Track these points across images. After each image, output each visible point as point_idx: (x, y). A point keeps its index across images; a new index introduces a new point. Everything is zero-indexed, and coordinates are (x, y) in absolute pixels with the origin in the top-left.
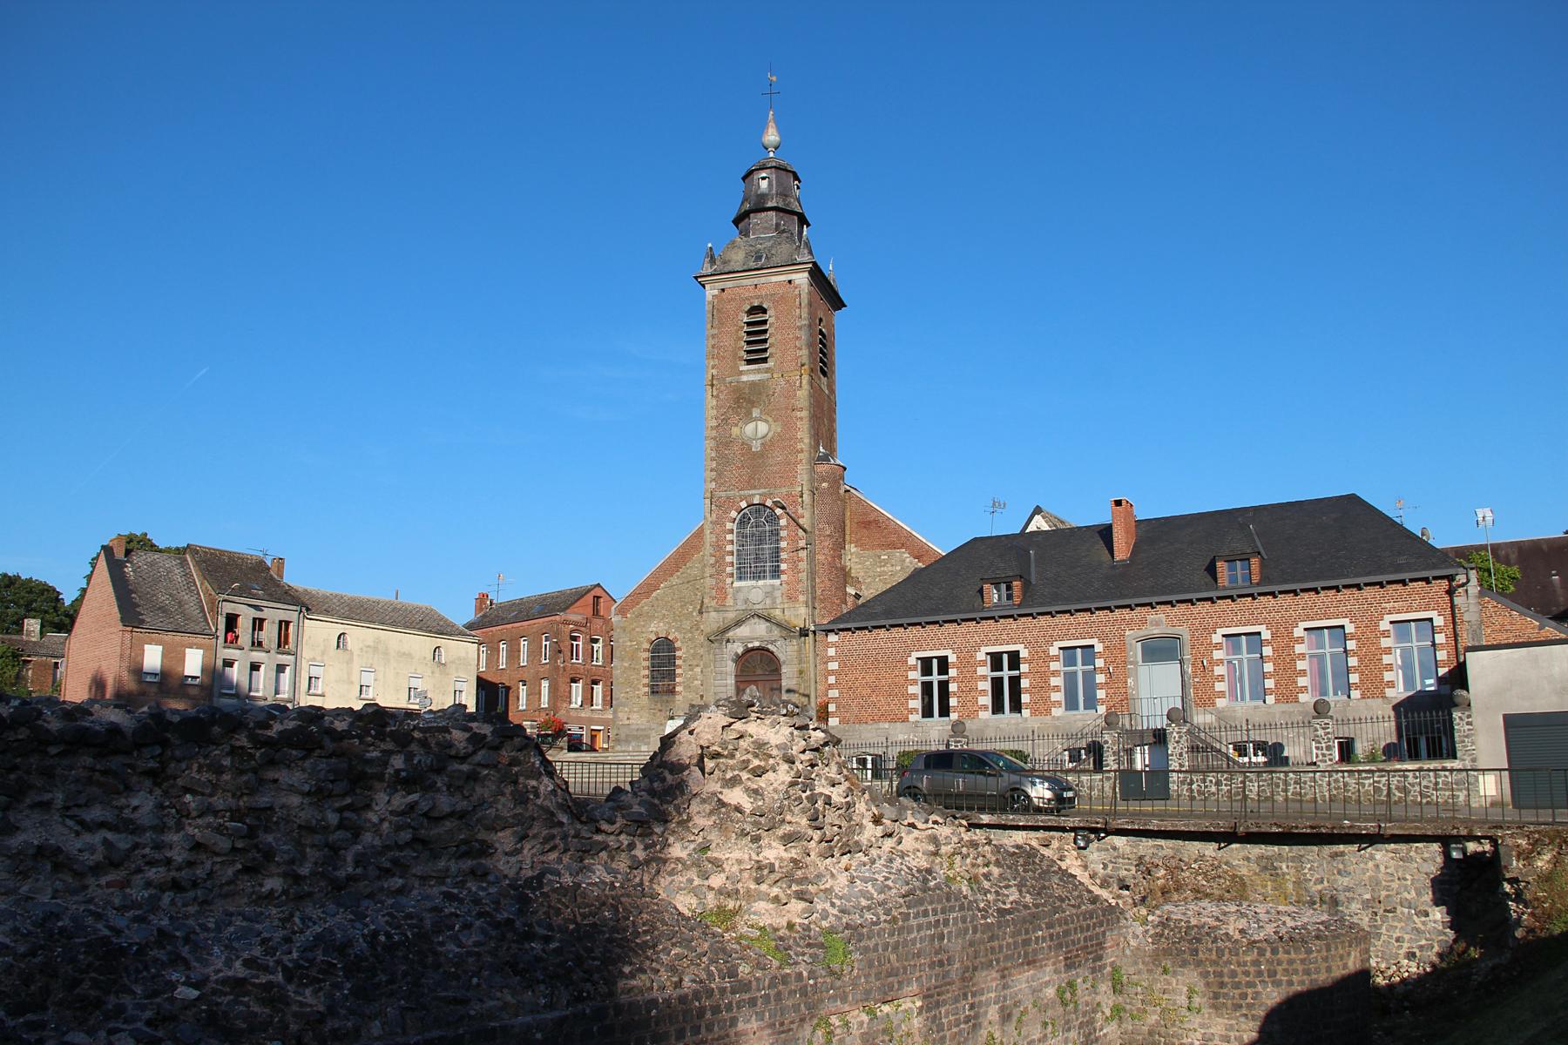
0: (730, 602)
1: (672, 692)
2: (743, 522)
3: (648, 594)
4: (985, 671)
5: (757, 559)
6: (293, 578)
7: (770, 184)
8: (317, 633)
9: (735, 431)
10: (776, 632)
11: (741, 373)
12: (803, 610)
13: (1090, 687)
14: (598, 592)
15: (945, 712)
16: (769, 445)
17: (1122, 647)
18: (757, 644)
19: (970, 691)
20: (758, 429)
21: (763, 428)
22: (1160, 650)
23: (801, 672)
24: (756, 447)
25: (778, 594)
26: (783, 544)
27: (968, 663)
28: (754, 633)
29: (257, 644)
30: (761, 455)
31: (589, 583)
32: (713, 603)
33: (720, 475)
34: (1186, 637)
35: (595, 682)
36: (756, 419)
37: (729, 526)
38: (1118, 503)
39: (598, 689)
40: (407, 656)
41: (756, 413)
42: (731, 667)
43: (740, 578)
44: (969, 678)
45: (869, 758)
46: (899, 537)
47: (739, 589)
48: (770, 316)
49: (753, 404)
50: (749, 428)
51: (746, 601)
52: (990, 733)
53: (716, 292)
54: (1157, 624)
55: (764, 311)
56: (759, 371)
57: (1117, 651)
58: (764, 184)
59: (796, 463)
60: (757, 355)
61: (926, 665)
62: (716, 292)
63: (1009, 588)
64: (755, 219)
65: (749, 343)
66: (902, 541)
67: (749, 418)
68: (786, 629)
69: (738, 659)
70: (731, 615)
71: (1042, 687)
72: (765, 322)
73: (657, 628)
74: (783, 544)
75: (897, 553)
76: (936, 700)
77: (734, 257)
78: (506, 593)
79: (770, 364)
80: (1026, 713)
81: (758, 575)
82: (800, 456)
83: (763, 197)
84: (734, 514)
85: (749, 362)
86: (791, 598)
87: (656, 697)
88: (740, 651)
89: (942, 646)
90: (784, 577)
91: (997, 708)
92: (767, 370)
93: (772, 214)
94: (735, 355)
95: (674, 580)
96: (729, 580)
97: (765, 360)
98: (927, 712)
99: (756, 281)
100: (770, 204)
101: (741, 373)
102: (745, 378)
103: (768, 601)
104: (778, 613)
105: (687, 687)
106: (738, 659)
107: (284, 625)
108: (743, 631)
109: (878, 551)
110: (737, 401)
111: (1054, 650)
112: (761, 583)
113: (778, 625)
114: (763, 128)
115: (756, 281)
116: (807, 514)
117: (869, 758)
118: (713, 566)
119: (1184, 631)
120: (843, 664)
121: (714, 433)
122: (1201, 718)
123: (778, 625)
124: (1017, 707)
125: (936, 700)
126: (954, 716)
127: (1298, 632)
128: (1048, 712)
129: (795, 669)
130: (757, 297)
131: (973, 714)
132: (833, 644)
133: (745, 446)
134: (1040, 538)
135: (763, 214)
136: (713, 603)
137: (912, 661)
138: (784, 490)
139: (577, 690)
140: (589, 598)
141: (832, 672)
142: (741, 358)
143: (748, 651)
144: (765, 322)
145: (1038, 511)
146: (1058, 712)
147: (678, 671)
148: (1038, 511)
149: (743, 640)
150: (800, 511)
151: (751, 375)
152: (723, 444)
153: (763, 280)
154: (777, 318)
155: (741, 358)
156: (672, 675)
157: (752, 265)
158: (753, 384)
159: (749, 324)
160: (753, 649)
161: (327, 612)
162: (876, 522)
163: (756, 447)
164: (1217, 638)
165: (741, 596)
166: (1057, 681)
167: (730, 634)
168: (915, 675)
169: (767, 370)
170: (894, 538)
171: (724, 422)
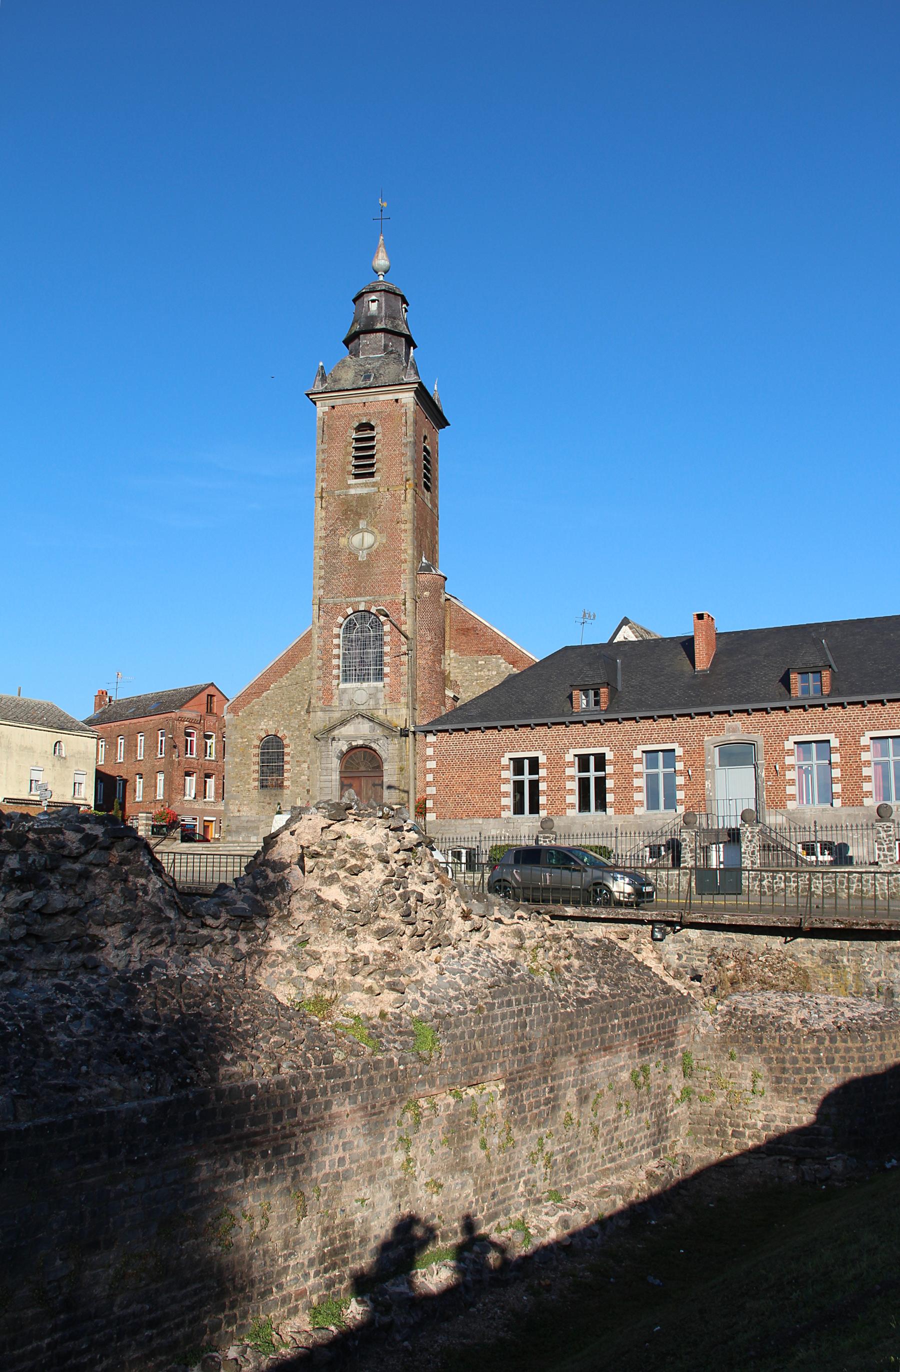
0: (335, 702)
1: (281, 786)
2: (350, 626)
3: (258, 694)
4: (573, 771)
5: (362, 662)
7: (379, 307)
9: (343, 541)
10: (379, 731)
11: (349, 486)
12: (404, 711)
14: (210, 690)
15: (535, 809)
16: (374, 555)
17: (701, 750)
18: (360, 742)
19: (558, 790)
20: (364, 540)
21: (369, 539)
22: (736, 754)
23: (401, 769)
24: (362, 556)
25: (381, 695)
26: (387, 649)
27: (557, 764)
28: (358, 732)
30: (368, 564)
31: (203, 682)
32: (320, 704)
33: (328, 583)
34: (761, 743)
35: (208, 776)
36: (362, 531)
37: (336, 630)
38: (700, 617)
39: (211, 782)
40: (28, 750)
41: (362, 524)
42: (336, 763)
43: (346, 680)
44: (557, 778)
45: (464, 851)
46: (495, 644)
47: (344, 691)
48: (378, 433)
49: (360, 516)
50: (356, 539)
51: (351, 702)
52: (576, 830)
53: (326, 409)
54: (734, 730)
55: (372, 428)
56: (366, 485)
57: (696, 755)
58: (374, 307)
59: (400, 573)
60: (364, 471)
61: (518, 766)
62: (326, 409)
63: (596, 694)
64: (365, 340)
65: (357, 458)
66: (500, 648)
67: (356, 530)
68: (388, 728)
69: (343, 756)
70: (337, 715)
71: (626, 788)
72: (372, 439)
73: (266, 726)
74: (387, 649)
75: (493, 659)
76: (527, 798)
77: (345, 376)
78: (122, 693)
79: (377, 478)
80: (610, 811)
81: (362, 678)
82: (404, 566)
83: (373, 319)
84: (340, 620)
85: (357, 476)
87: (265, 791)
88: (345, 748)
89: (533, 748)
90: (387, 680)
91: (584, 806)
92: (374, 485)
93: (381, 335)
94: (343, 469)
95: (284, 681)
96: (335, 682)
97: (372, 475)
98: (518, 809)
99: (364, 399)
100: (379, 326)
101: (349, 486)
102: (352, 491)
103: (372, 702)
104: (380, 713)
105: (295, 782)
106: (343, 756)
108: (348, 730)
109: (476, 657)
110: (345, 513)
111: (637, 754)
112: (365, 685)
113: (381, 724)
114: (374, 253)
115: (364, 399)
116: (409, 621)
117: (464, 851)
118: (320, 668)
119: (758, 738)
120: (440, 764)
121: (323, 543)
122: (773, 819)
123: (381, 724)
124: (602, 805)
125: (527, 798)
126: (543, 813)
127: (865, 741)
128: (631, 810)
129: (396, 766)
130: (366, 415)
131: (561, 812)
132: (432, 745)
133: (353, 555)
134: (627, 647)
135: (373, 336)
136: (320, 704)
137: (505, 761)
138: (388, 598)
139: (191, 783)
140: (203, 696)
141: (431, 771)
142: (349, 473)
143: (352, 749)
144: (372, 439)
145: (625, 622)
146: (640, 811)
147: (286, 767)
149: (349, 739)
150: (403, 618)
151: (358, 488)
152: (331, 553)
153: (371, 398)
154: (384, 435)
155: (349, 473)
156: (280, 771)
157: (361, 383)
158: (360, 498)
159: (357, 440)
160: (357, 747)
162: (474, 629)
163: (362, 556)
164: (789, 745)
165: (346, 697)
166: (640, 782)
167: (336, 733)
168: (508, 774)
169: (374, 485)
170: (491, 645)
171: (332, 532)
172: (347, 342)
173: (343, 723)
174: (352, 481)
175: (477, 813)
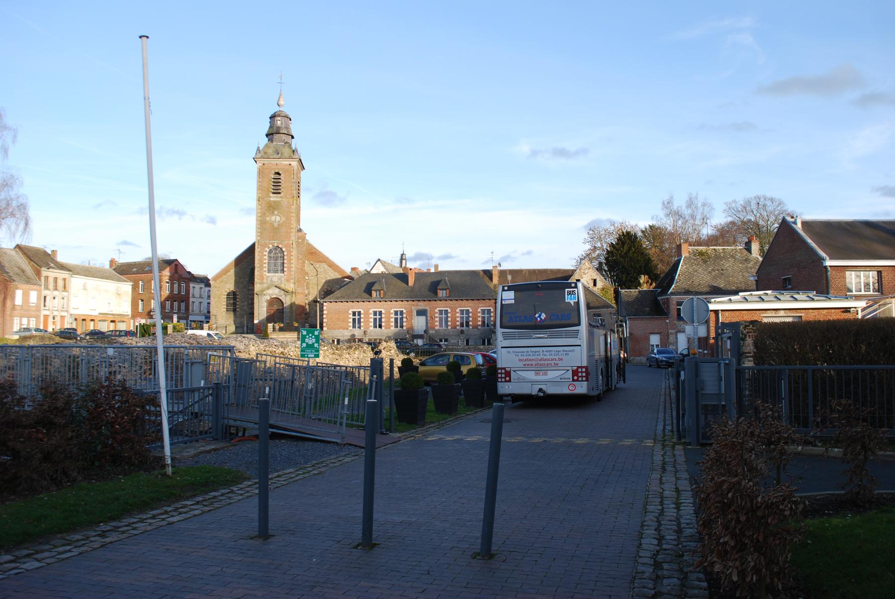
2: (270, 252)
3: (225, 274)
4: (372, 316)
6: (60, 258)
8: (77, 282)
9: (268, 219)
10: (282, 292)
12: (292, 285)
13: (402, 322)
15: (360, 327)
19: (367, 322)
21: (278, 218)
22: (421, 313)
24: (276, 225)
27: (367, 313)
29: (56, 289)
30: (278, 228)
41: (276, 213)
42: (265, 304)
44: (367, 318)
50: (273, 218)
61: (354, 314)
64: (276, 136)
66: (332, 265)
70: (265, 285)
76: (357, 323)
78: (123, 259)
79: (282, 195)
81: (276, 272)
83: (278, 128)
86: (288, 281)
91: (375, 327)
106: (267, 301)
107: (65, 280)
108: (270, 291)
119: (428, 308)
122: (431, 332)
124: (380, 326)
125: (357, 323)
133: (272, 224)
148: (379, 260)
149: (269, 295)
151: (274, 198)
161: (78, 274)
163: (276, 225)
165: (269, 279)
168: (351, 316)
172: (267, 135)
173: (268, 288)
174: (272, 195)
175: (341, 328)
